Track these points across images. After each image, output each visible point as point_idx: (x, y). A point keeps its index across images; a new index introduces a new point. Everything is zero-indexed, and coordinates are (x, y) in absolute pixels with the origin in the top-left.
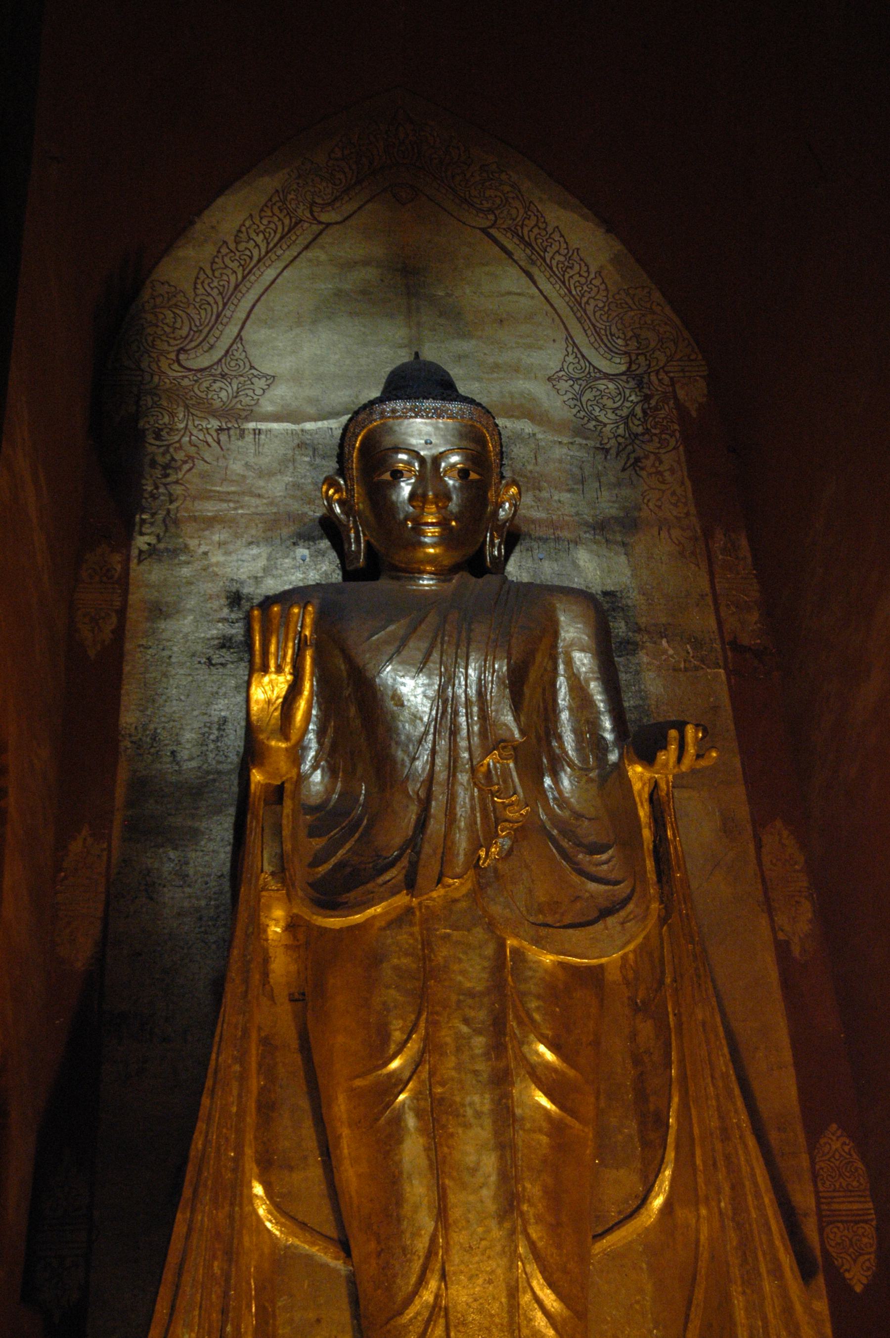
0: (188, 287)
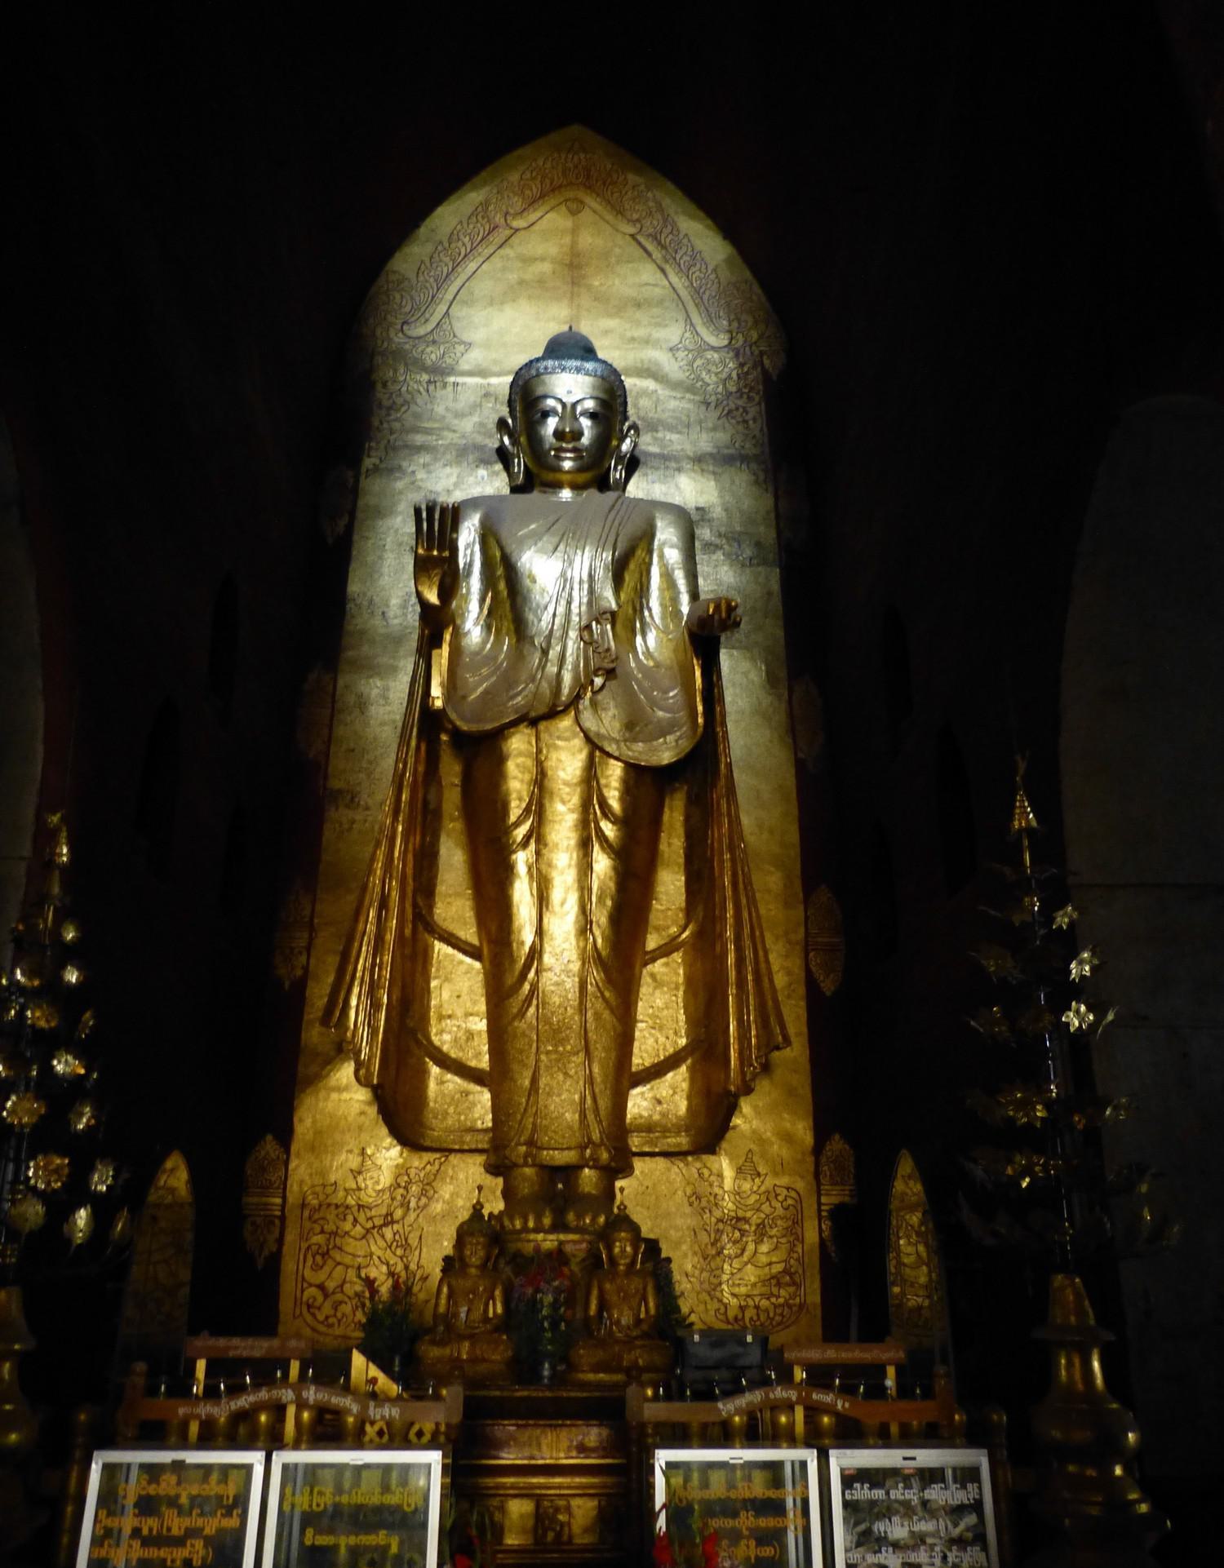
0: (412, 275)
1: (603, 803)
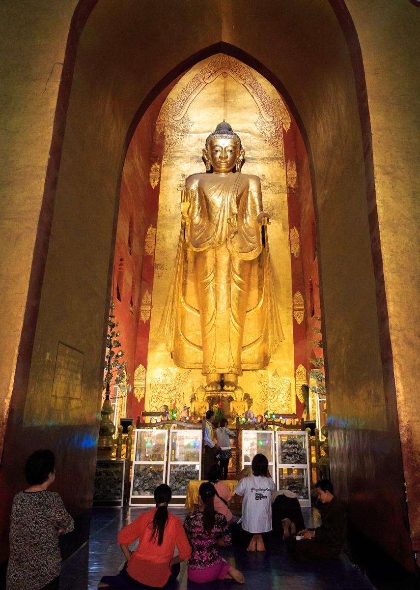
0: (175, 100)
1: (234, 271)
